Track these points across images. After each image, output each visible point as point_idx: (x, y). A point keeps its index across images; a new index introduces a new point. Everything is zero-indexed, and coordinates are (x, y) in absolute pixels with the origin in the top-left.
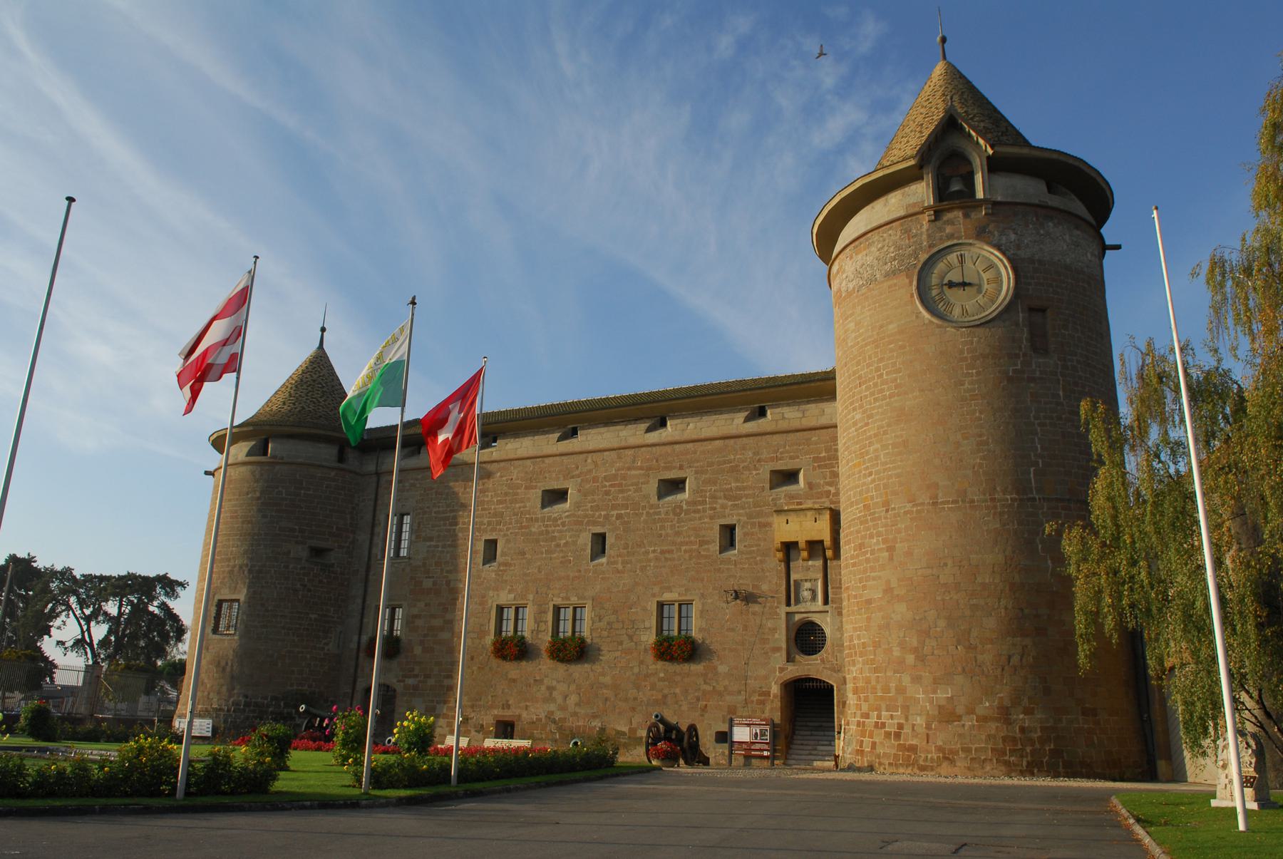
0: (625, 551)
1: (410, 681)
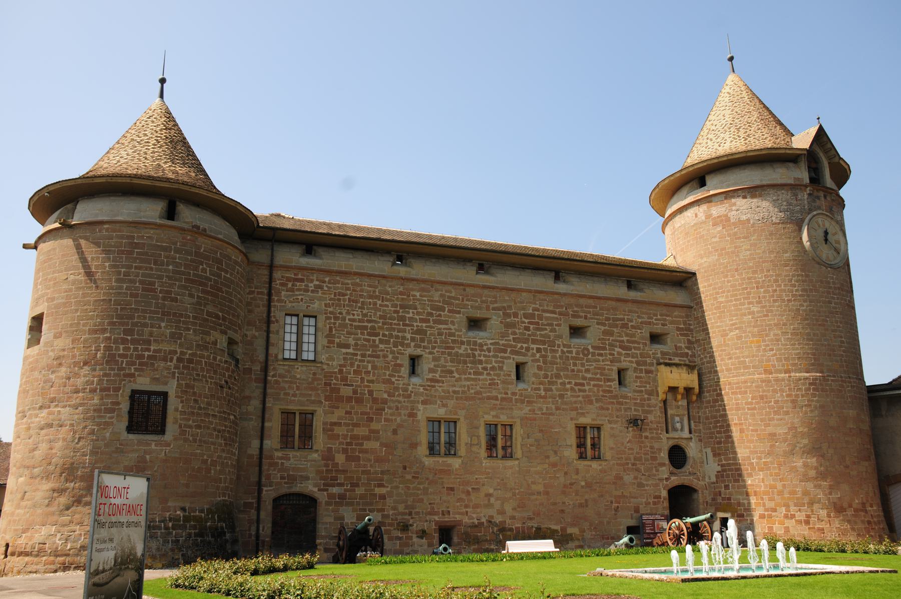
0: (546, 380)
1: (335, 490)
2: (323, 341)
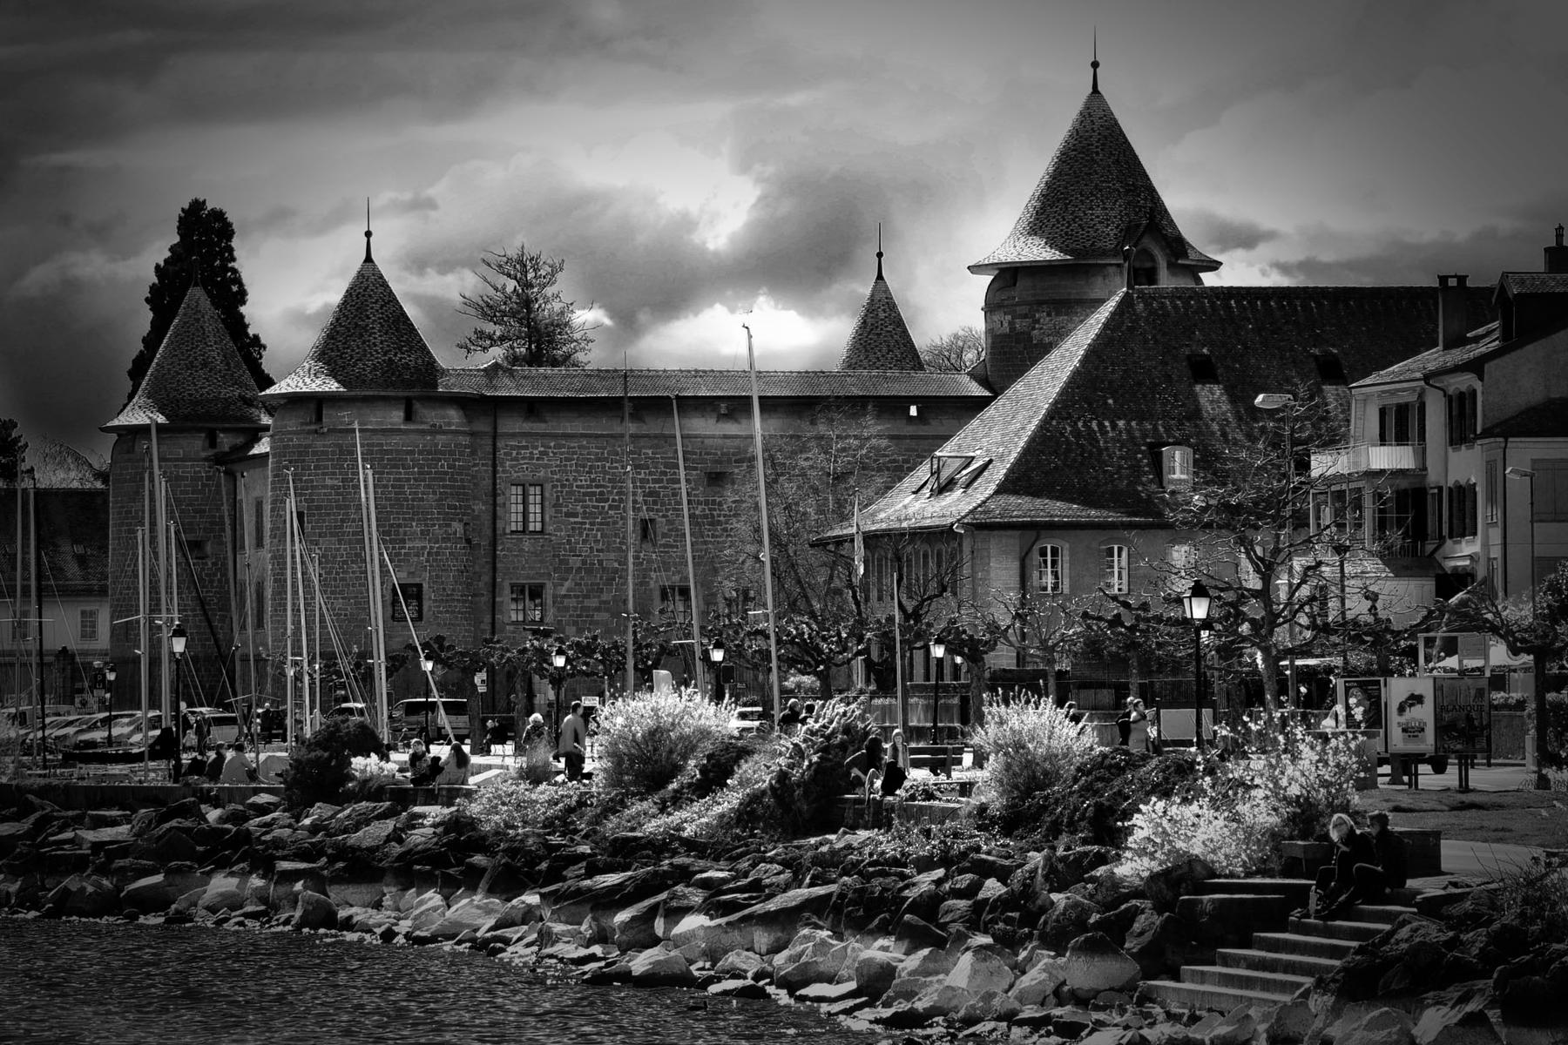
2: (549, 512)
